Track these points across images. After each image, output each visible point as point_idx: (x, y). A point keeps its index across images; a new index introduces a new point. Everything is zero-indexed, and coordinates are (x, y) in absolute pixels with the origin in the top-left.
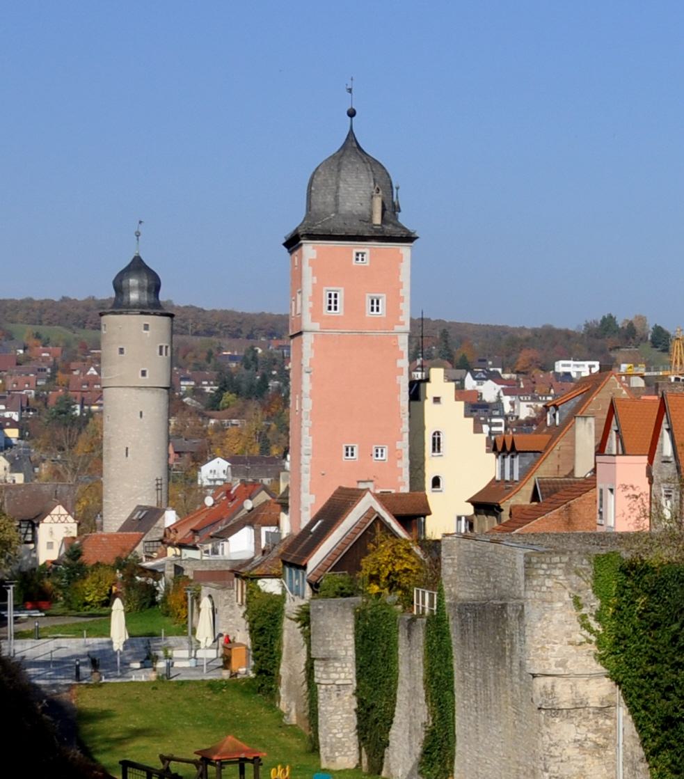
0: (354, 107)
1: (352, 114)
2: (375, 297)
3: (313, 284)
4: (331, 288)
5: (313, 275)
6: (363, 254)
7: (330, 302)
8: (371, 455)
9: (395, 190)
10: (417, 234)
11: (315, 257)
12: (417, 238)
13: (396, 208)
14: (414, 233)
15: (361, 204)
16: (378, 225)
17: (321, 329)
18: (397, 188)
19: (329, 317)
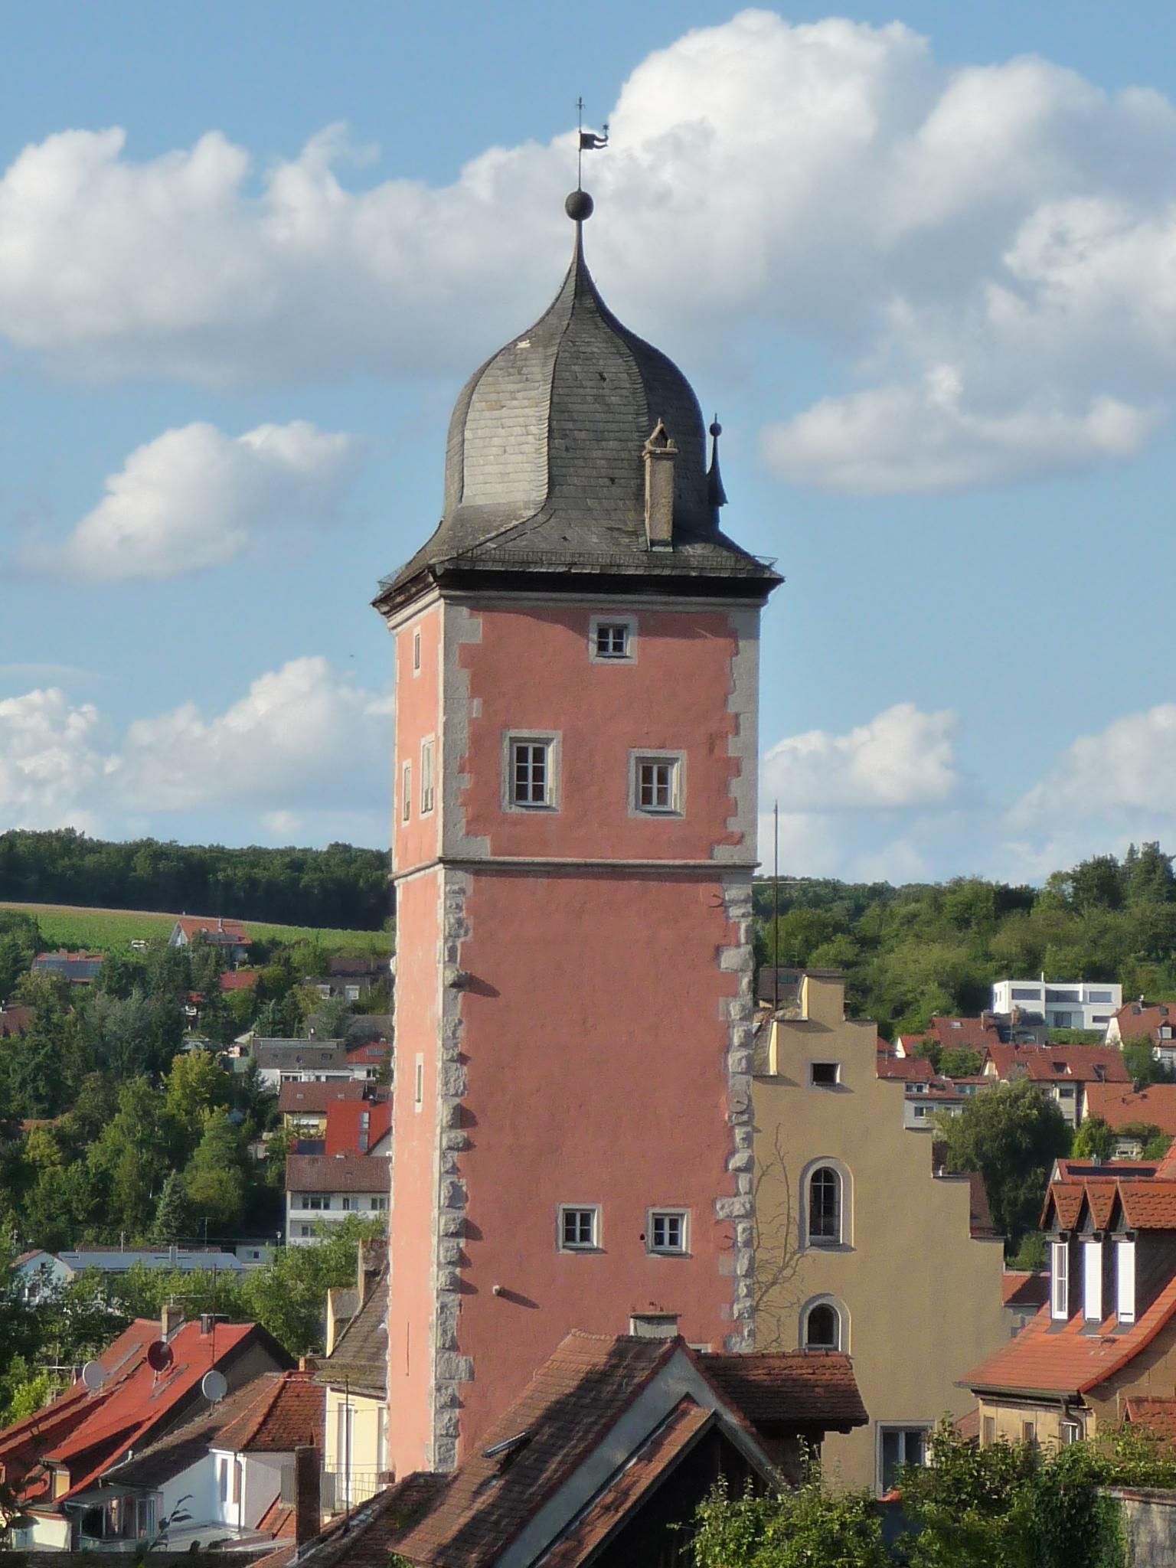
0: (583, 190)
1: (581, 207)
2: (656, 760)
3: (472, 721)
4: (525, 733)
5: (472, 697)
6: (620, 632)
7: (522, 773)
8: (642, 1238)
9: (709, 439)
10: (778, 569)
11: (478, 639)
12: (780, 580)
13: (714, 495)
14: (768, 567)
15: (612, 480)
16: (664, 544)
17: (494, 854)
18: (715, 430)
19: (517, 822)
